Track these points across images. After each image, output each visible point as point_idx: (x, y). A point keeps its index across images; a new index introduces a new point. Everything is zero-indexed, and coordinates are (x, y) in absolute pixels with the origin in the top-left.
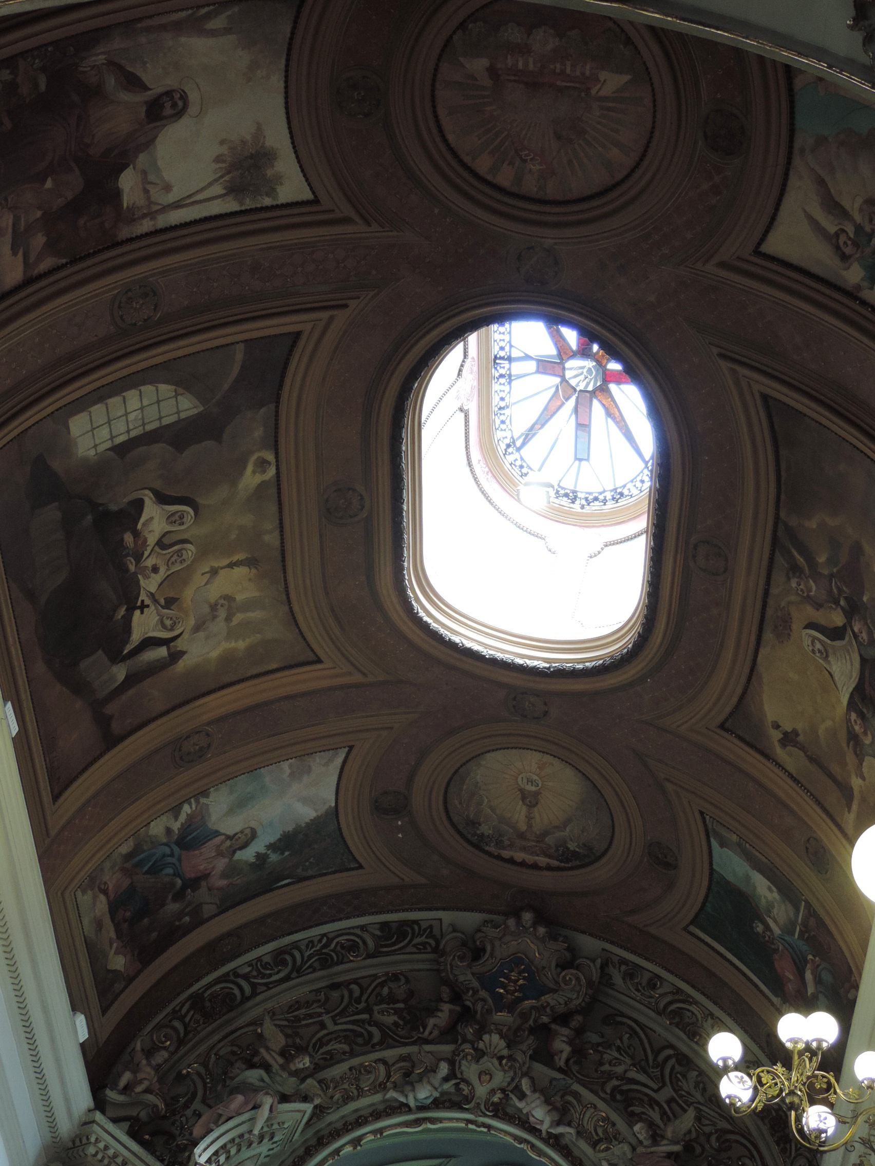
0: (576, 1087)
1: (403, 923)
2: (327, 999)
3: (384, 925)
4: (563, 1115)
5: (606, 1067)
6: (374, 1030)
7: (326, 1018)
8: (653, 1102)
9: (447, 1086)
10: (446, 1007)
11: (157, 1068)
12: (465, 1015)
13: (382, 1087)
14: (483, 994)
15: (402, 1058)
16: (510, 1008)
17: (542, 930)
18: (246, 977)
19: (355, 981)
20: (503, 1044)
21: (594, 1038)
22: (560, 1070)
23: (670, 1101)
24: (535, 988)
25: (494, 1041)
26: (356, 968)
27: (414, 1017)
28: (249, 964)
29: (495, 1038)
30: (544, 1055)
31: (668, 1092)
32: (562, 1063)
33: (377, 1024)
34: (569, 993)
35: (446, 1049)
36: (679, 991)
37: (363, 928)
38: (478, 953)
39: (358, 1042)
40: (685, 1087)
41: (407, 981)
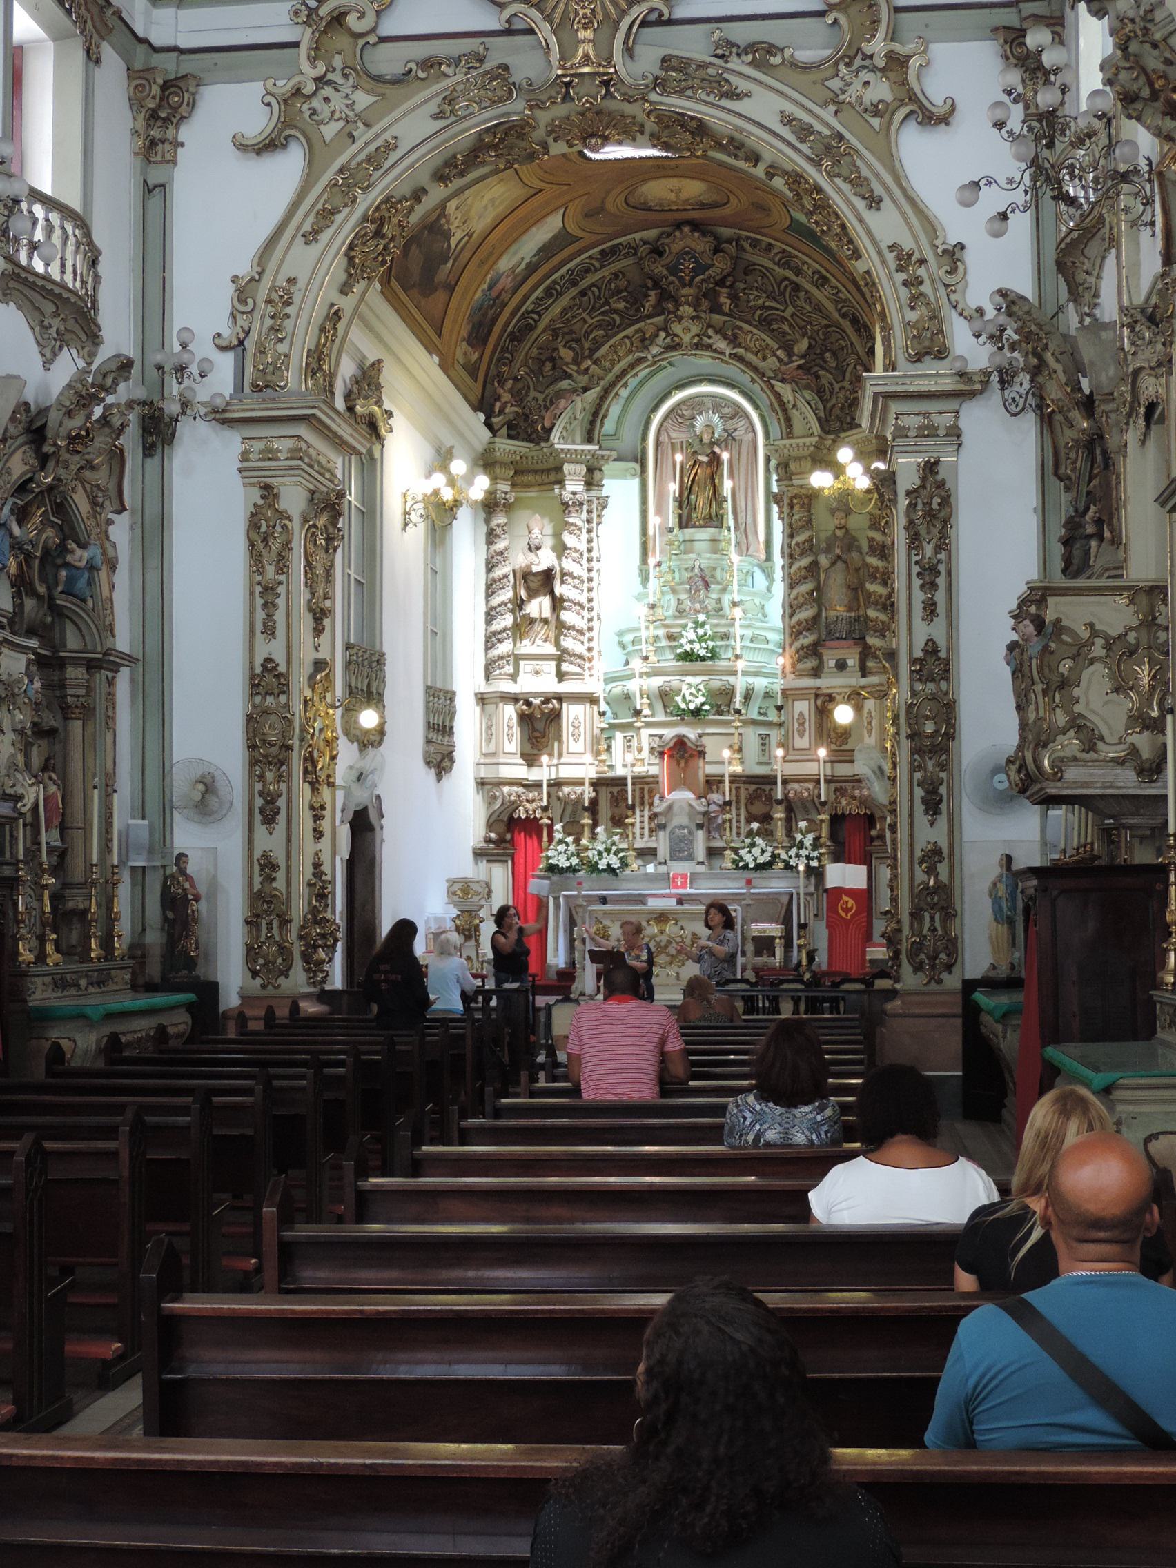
0: (739, 323)
1: (613, 246)
2: (581, 302)
3: (602, 252)
4: (733, 341)
5: (752, 303)
6: (615, 316)
7: (584, 315)
8: (784, 319)
9: (668, 339)
10: (652, 293)
11: (510, 391)
12: (665, 296)
13: (630, 351)
14: (671, 278)
15: (637, 331)
16: (690, 285)
17: (696, 234)
18: (532, 312)
19: (593, 285)
20: (691, 309)
21: (742, 286)
22: (726, 315)
23: (792, 316)
24: (700, 268)
25: (687, 310)
26: (590, 279)
27: (636, 300)
28: (533, 303)
29: (686, 307)
30: (716, 308)
31: (790, 310)
32: (727, 310)
33: (615, 311)
34: (720, 265)
35: (660, 319)
36: (784, 251)
37: (590, 257)
38: (661, 254)
39: (611, 328)
40: (798, 302)
41: (624, 275)
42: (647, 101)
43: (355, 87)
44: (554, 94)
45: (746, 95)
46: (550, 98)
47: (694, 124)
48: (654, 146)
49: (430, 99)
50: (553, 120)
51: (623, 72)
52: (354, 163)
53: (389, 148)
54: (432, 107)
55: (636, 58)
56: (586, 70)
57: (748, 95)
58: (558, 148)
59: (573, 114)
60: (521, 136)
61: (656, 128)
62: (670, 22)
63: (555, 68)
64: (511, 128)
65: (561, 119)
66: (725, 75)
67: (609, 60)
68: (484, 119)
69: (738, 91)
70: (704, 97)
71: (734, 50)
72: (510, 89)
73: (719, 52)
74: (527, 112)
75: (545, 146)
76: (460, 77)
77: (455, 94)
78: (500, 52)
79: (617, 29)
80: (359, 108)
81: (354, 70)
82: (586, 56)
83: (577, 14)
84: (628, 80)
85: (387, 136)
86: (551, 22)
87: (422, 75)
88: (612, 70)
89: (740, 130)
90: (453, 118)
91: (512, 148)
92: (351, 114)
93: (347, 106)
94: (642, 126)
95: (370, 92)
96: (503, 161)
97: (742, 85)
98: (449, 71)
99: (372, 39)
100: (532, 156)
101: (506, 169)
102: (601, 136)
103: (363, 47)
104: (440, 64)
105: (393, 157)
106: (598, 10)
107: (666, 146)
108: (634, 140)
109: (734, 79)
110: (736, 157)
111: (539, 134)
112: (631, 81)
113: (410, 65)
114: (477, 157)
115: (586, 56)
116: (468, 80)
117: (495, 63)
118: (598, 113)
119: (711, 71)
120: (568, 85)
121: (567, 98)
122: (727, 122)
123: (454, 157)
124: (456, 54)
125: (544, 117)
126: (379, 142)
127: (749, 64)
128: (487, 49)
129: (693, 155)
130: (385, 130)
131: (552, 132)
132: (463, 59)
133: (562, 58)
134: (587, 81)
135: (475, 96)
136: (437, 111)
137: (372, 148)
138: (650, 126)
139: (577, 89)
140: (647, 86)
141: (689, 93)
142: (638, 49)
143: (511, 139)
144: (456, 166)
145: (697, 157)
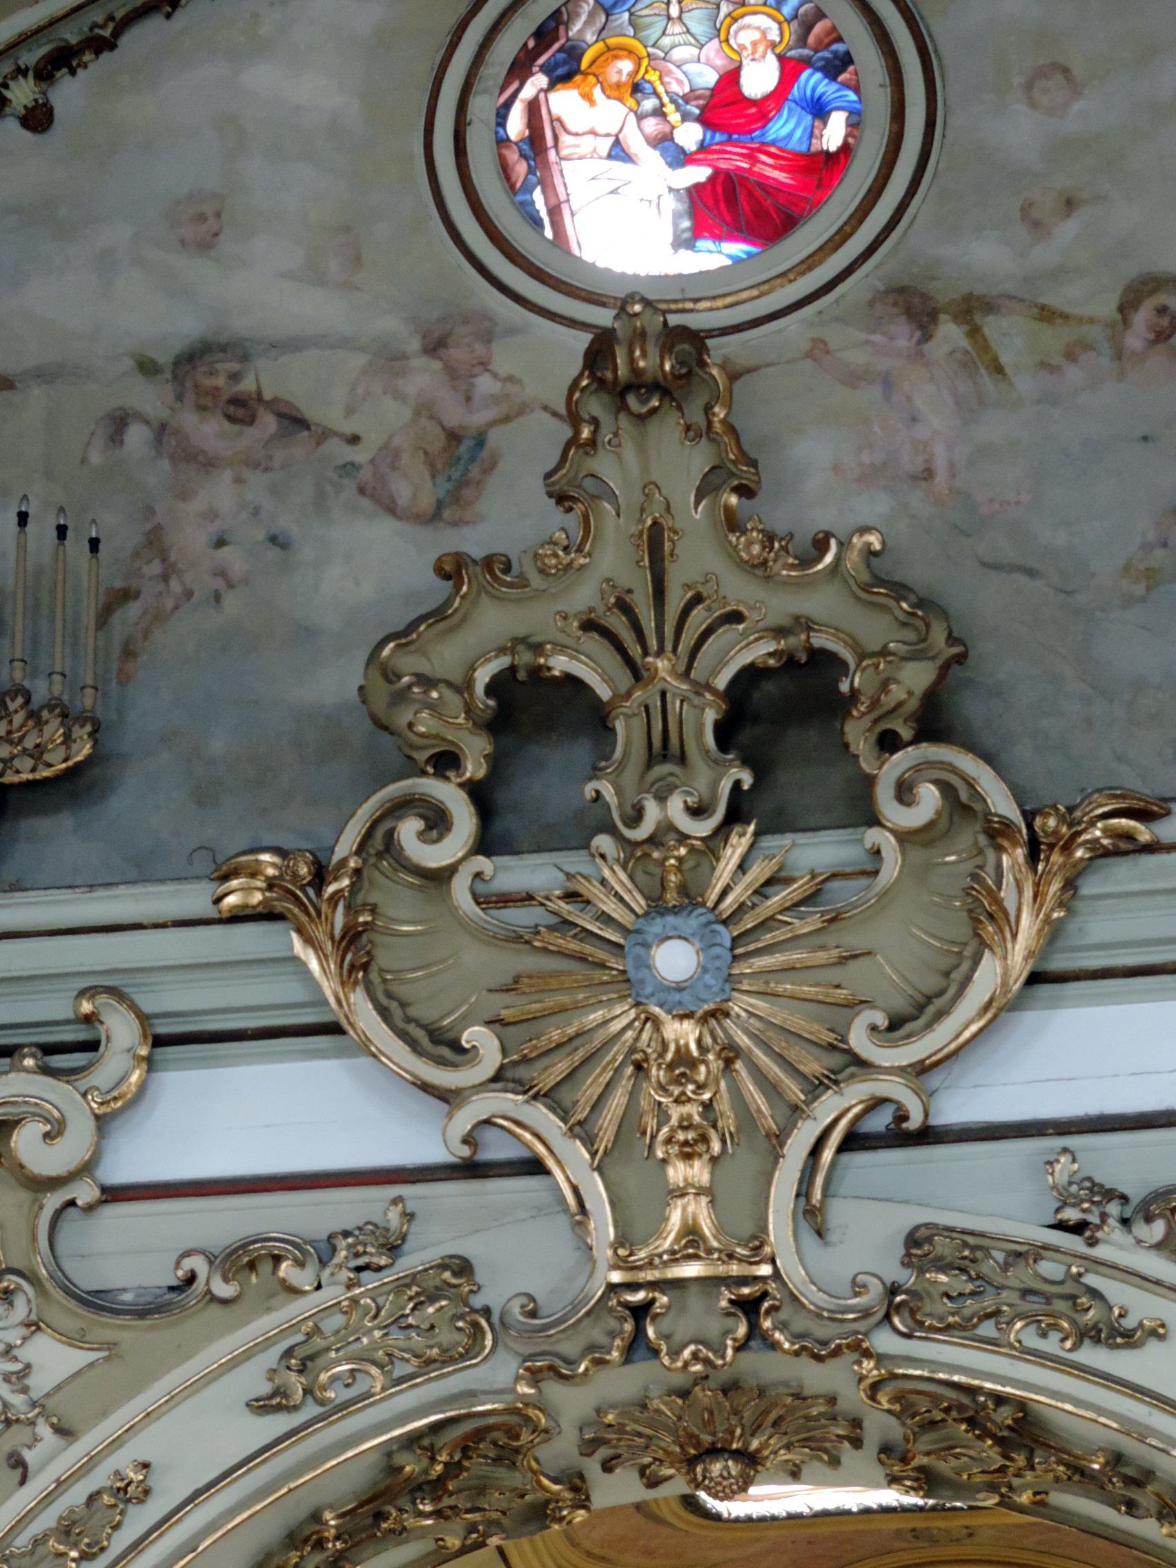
42: (867, 1354)
43: (33, 1326)
44: (602, 1339)
45: (1153, 1333)
46: (591, 1348)
47: (1005, 1415)
48: (893, 1480)
49: (248, 1355)
50: (599, 1411)
51: (794, 1273)
52: (23, 1541)
53: (127, 1494)
54: (253, 1380)
55: (832, 1237)
56: (691, 1270)
57: (1157, 1333)
58: (616, 1490)
59: (655, 1391)
60: (508, 1456)
61: (895, 1430)
62: (928, 1136)
63: (602, 1265)
64: (479, 1435)
65: (624, 1409)
66: (1091, 1280)
67: (757, 1246)
68: (409, 1407)
69: (1129, 1323)
70: (1031, 1339)
71: (1113, 1208)
72: (477, 1326)
73: (1072, 1215)
74: (524, 1389)
75: (577, 1485)
76: (333, 1293)
77: (318, 1342)
78: (447, 1223)
79: (776, 1157)
80: (41, 1383)
81: (33, 1279)
82: (691, 1233)
83: (662, 1115)
84: (812, 1296)
85: (123, 1460)
86: (589, 1142)
87: (223, 1289)
88: (765, 1270)
89: (1141, 1433)
90: (311, 1410)
91: (481, 1490)
92: (17, 1400)
93: (7, 1378)
94: (856, 1423)
95: (74, 1340)
96: (457, 1525)
97: (1143, 1308)
98: (302, 1278)
99: (85, 1193)
100: (540, 1514)
101: (464, 1550)
102: (738, 1455)
103: (58, 1214)
104: (277, 1259)
105: (139, 1520)
106: (724, 1105)
107: (927, 1481)
108: (835, 1462)
109: (1116, 1291)
110: (1131, 1507)
111: (561, 1449)
112: (822, 1299)
113: (188, 1264)
114: (380, 1516)
115: (691, 1233)
116: (354, 1301)
117: (434, 1254)
118: (730, 1388)
119: (1049, 1268)
120: (640, 1312)
121: (637, 1346)
122: (1100, 1411)
123: (316, 1517)
124: (321, 1231)
125: (572, 1404)
126: (99, 1478)
127: (1158, 1246)
128: (409, 1216)
129: (1006, 1503)
130: (116, 1444)
131: (596, 1443)
132: (342, 1243)
133: (620, 1242)
134: (694, 1300)
135: (374, 1346)
136: (265, 1388)
137: (76, 1496)
138: (880, 1423)
139: (666, 1324)
140: (866, 1313)
141: (987, 1329)
142: (840, 1213)
143: (477, 1466)
144: (320, 1544)
145: (1021, 1509)
